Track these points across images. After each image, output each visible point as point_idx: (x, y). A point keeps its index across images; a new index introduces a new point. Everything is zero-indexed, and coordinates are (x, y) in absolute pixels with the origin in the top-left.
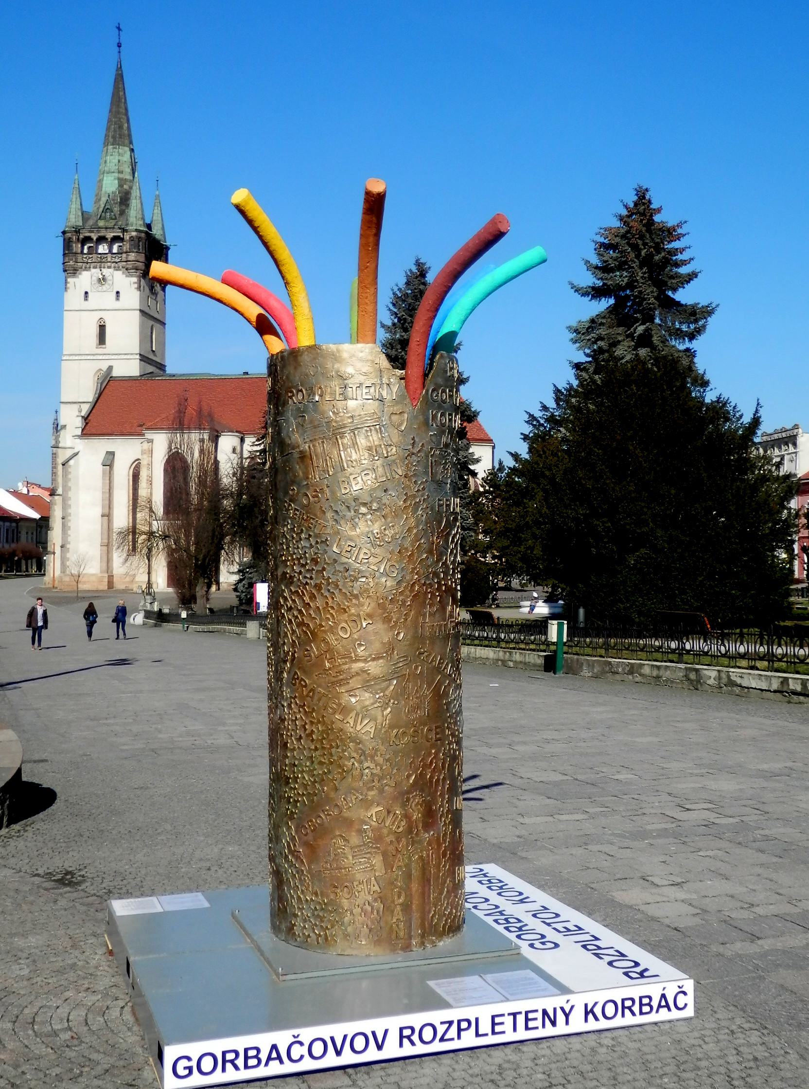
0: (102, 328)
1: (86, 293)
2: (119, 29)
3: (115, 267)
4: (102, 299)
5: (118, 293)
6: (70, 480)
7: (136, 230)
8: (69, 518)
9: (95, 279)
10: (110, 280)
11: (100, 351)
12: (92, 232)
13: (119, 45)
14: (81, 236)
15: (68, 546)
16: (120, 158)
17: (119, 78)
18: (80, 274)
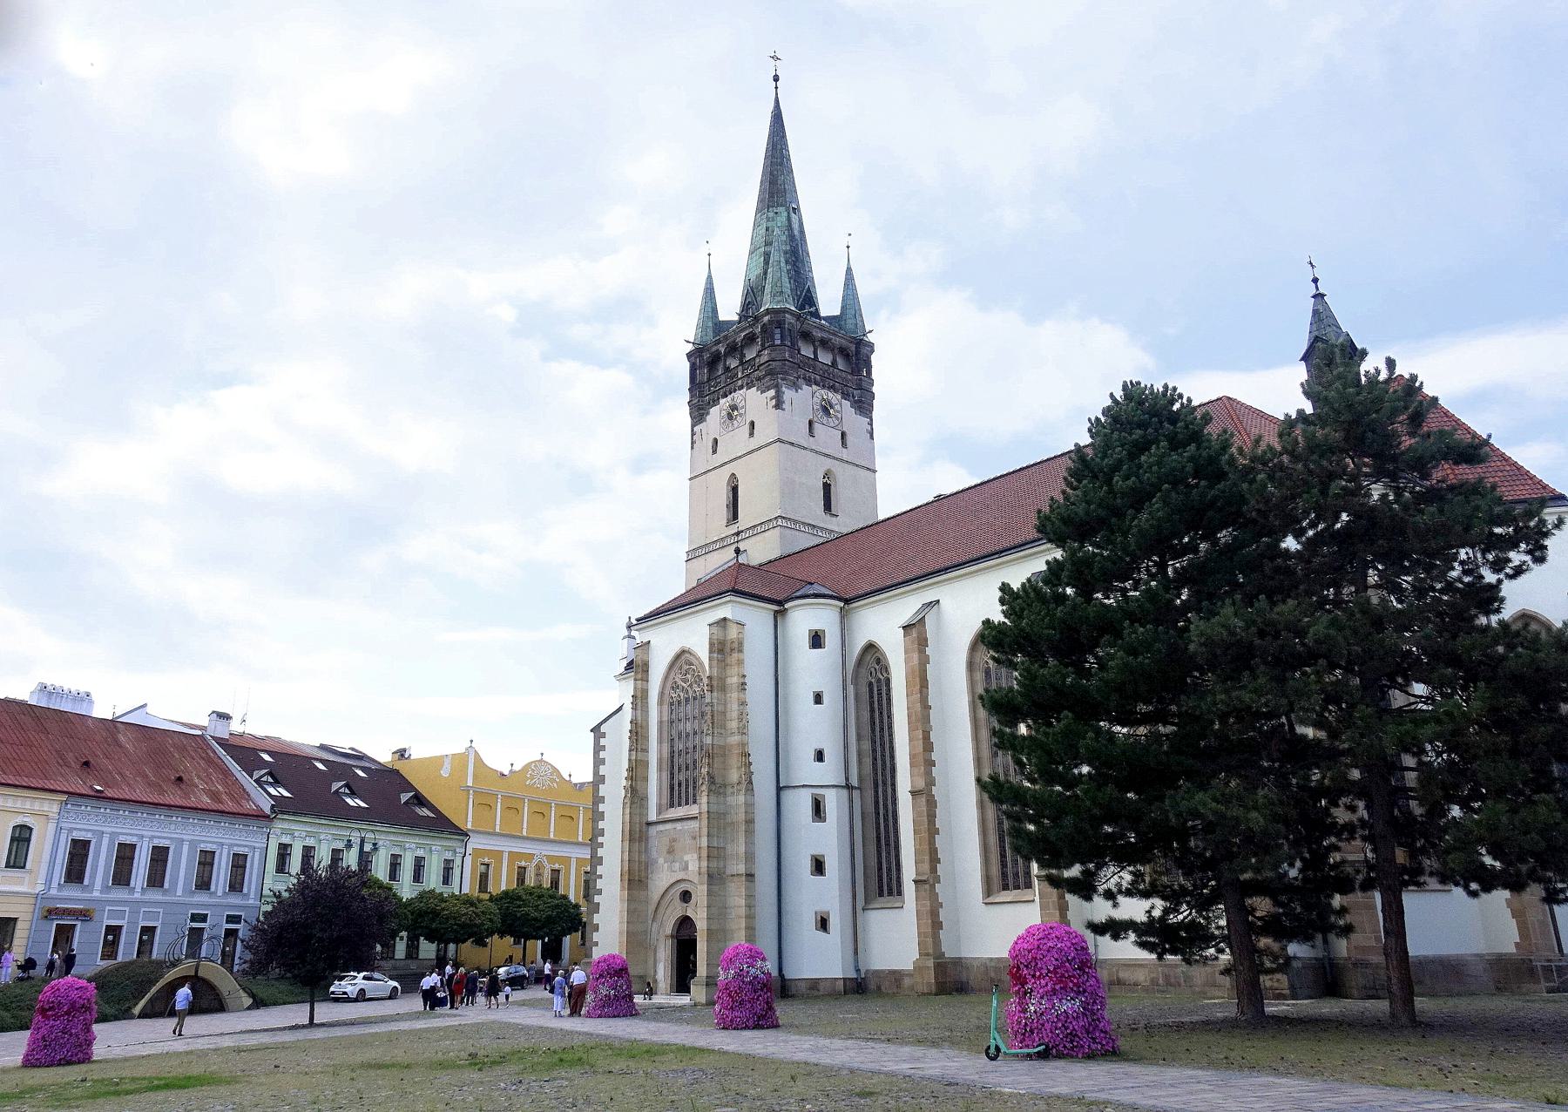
0: (735, 490)
1: (716, 441)
2: (775, 58)
3: (747, 384)
4: (736, 441)
5: (752, 424)
6: (603, 762)
7: (768, 311)
8: (600, 840)
9: (724, 413)
10: (742, 407)
11: (734, 529)
12: (718, 342)
13: (776, 79)
14: (706, 356)
15: (597, 899)
16: (770, 224)
17: (777, 118)
18: (708, 413)
